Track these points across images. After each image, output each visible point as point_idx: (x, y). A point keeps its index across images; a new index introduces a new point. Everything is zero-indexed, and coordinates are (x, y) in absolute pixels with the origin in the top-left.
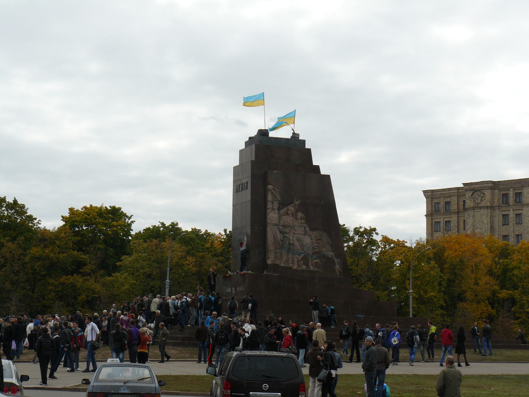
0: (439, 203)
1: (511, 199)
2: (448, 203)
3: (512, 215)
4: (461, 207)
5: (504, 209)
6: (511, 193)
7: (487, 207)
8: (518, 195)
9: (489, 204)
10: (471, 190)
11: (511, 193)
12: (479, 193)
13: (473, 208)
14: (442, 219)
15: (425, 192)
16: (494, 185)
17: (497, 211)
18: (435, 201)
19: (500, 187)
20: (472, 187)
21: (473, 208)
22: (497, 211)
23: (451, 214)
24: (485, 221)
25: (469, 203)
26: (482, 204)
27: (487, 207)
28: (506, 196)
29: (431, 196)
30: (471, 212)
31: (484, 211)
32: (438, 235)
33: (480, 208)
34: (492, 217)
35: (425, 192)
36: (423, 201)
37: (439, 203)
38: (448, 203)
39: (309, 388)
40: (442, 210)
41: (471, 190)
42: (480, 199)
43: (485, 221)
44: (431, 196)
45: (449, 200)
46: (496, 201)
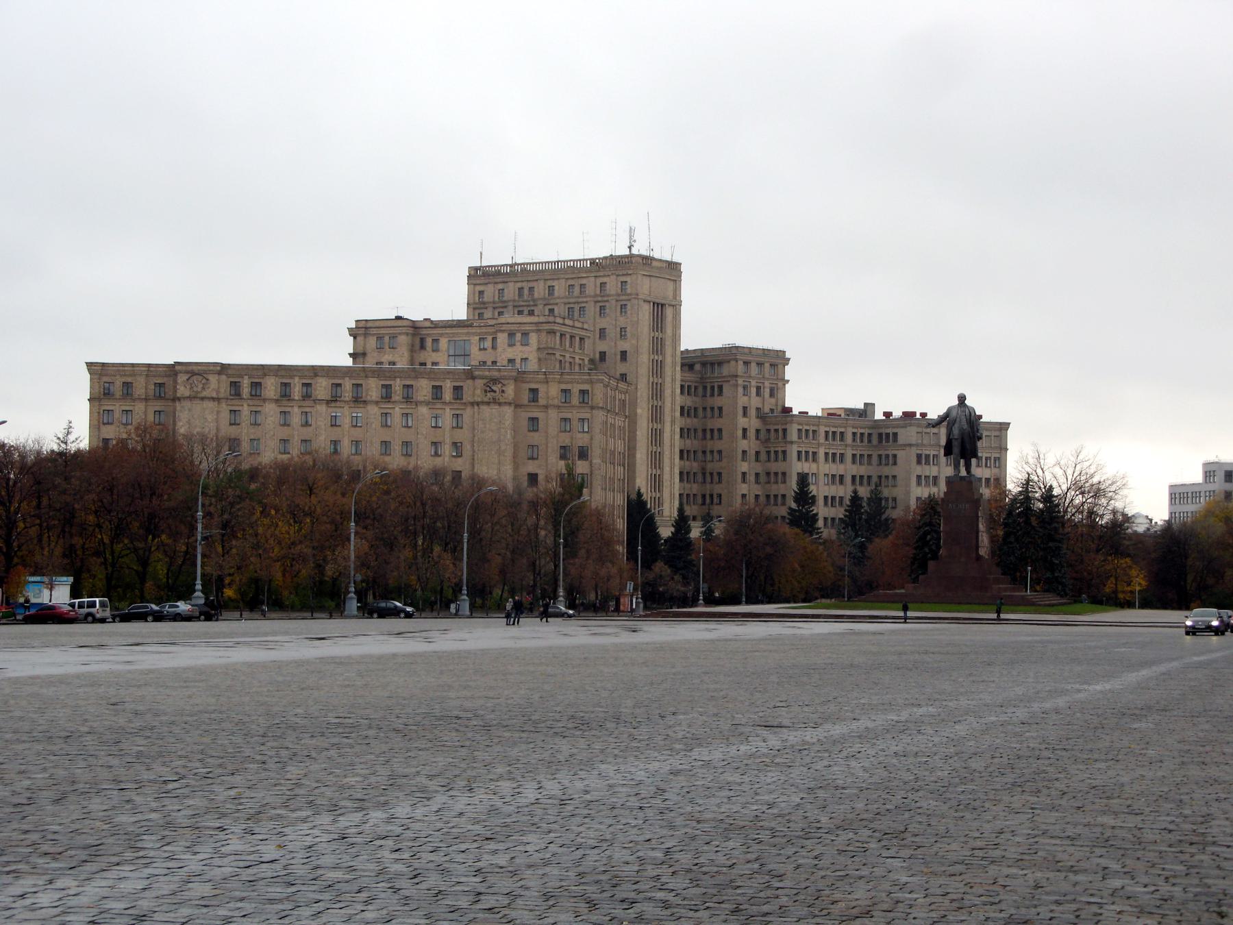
0: (110, 384)
1: (246, 391)
2: (127, 385)
3: (245, 410)
4: (151, 393)
5: (234, 402)
6: (246, 383)
7: (213, 399)
8: (256, 385)
9: (214, 395)
10: (187, 372)
11: (246, 383)
12: (200, 378)
13: (190, 398)
14: (117, 407)
15: (90, 365)
16: (223, 369)
17: (224, 405)
18: (105, 379)
19: (230, 372)
20: (190, 368)
21: (190, 398)
22: (224, 405)
23: (134, 400)
24: (210, 418)
25: (182, 391)
26: (204, 394)
27: (213, 399)
28: (235, 386)
29: (98, 370)
30: (187, 404)
31: (210, 404)
32: (110, 432)
33: (203, 399)
34: (218, 412)
35: (90, 365)
36: (87, 376)
37: (110, 384)
38: (127, 385)
39: (265, 645)
40: (118, 394)
41: (187, 372)
42: (200, 386)
43: (210, 418)
44: (98, 370)
45: (129, 380)
46: (222, 390)
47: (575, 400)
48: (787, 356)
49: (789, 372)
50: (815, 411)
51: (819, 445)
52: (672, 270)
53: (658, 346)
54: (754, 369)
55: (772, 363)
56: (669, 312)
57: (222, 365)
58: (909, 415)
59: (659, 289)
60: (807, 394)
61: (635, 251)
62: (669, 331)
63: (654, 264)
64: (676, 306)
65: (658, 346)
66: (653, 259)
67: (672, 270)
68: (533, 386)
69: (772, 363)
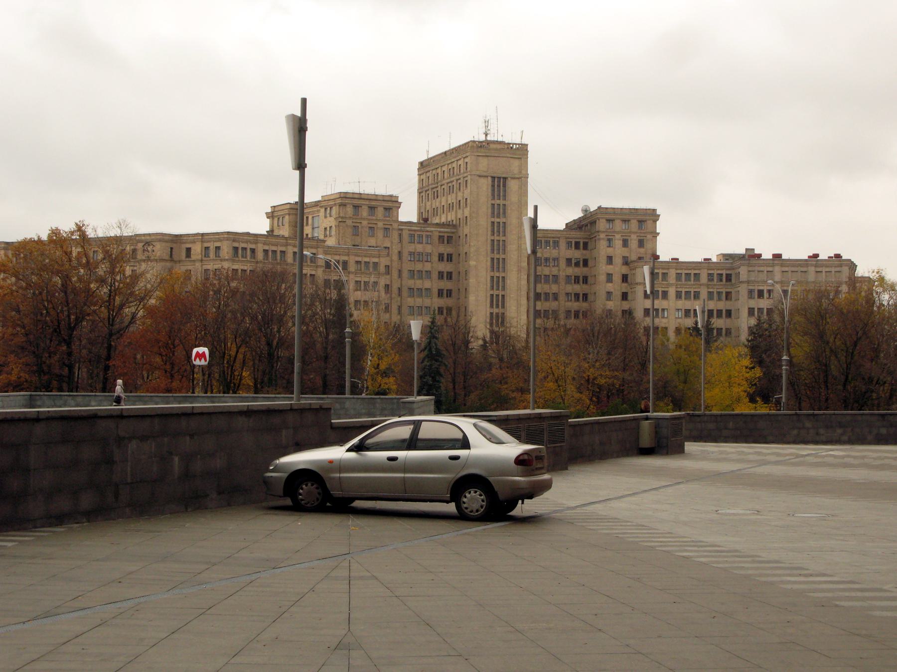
47: (212, 254)
48: (658, 213)
49: (660, 226)
50: (692, 254)
51: (669, 285)
52: (520, 152)
53: (498, 211)
54: (618, 225)
55: (645, 220)
56: (513, 185)
57: (7, 243)
58: (777, 256)
59: (499, 167)
60: (678, 242)
61: (489, 138)
62: (513, 197)
63: (492, 146)
64: (522, 178)
65: (498, 211)
66: (489, 143)
67: (520, 152)
68: (188, 246)
69: (645, 220)
